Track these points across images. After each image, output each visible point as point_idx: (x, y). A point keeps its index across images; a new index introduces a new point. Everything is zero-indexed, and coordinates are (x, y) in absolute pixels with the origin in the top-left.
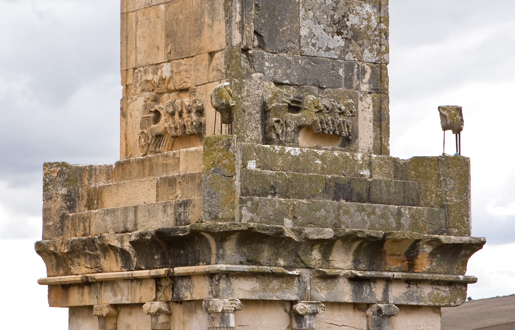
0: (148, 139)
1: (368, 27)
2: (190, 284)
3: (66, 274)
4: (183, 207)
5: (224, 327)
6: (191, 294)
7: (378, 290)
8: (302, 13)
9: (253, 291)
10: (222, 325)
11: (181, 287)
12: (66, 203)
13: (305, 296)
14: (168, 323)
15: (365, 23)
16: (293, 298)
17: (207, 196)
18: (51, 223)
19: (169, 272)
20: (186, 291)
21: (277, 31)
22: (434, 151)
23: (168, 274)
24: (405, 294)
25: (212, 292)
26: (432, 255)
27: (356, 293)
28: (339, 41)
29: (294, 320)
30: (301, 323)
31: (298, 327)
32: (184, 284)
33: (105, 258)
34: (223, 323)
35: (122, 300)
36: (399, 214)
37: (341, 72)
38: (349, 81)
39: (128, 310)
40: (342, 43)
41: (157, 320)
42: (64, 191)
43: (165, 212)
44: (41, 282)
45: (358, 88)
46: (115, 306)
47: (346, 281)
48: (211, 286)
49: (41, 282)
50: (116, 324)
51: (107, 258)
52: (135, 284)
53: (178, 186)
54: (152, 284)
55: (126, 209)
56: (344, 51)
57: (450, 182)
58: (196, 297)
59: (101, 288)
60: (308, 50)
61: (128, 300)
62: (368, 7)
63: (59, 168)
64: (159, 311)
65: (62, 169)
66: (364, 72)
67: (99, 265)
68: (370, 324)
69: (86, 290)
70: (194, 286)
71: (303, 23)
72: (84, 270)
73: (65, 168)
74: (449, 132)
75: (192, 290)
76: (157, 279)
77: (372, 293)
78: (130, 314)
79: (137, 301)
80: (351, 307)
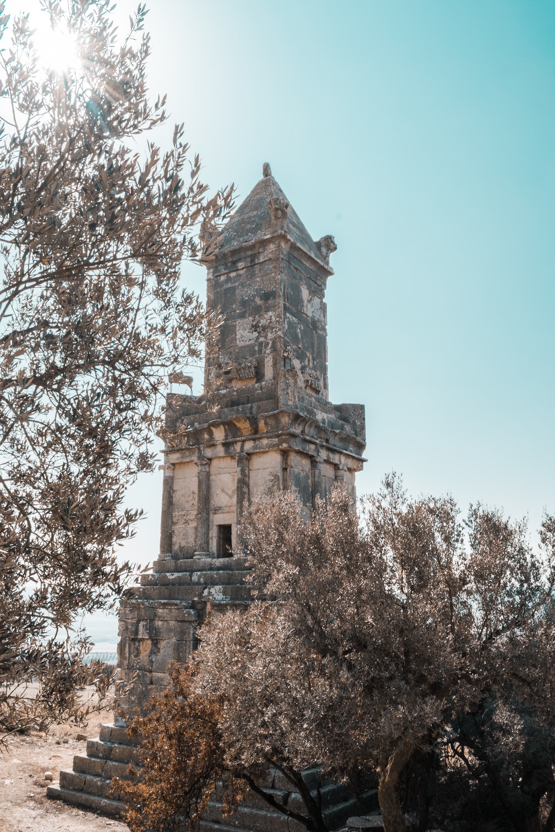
1: (270, 323)
7: (238, 447)
8: (238, 328)
9: (178, 458)
15: (269, 321)
21: (225, 341)
26: (266, 424)
28: (256, 334)
36: (251, 408)
37: (256, 348)
38: (260, 351)
40: (257, 334)
45: (265, 353)
56: (258, 338)
60: (240, 344)
62: (270, 313)
66: (268, 344)
71: (238, 333)
77: (235, 450)
80: (229, 458)
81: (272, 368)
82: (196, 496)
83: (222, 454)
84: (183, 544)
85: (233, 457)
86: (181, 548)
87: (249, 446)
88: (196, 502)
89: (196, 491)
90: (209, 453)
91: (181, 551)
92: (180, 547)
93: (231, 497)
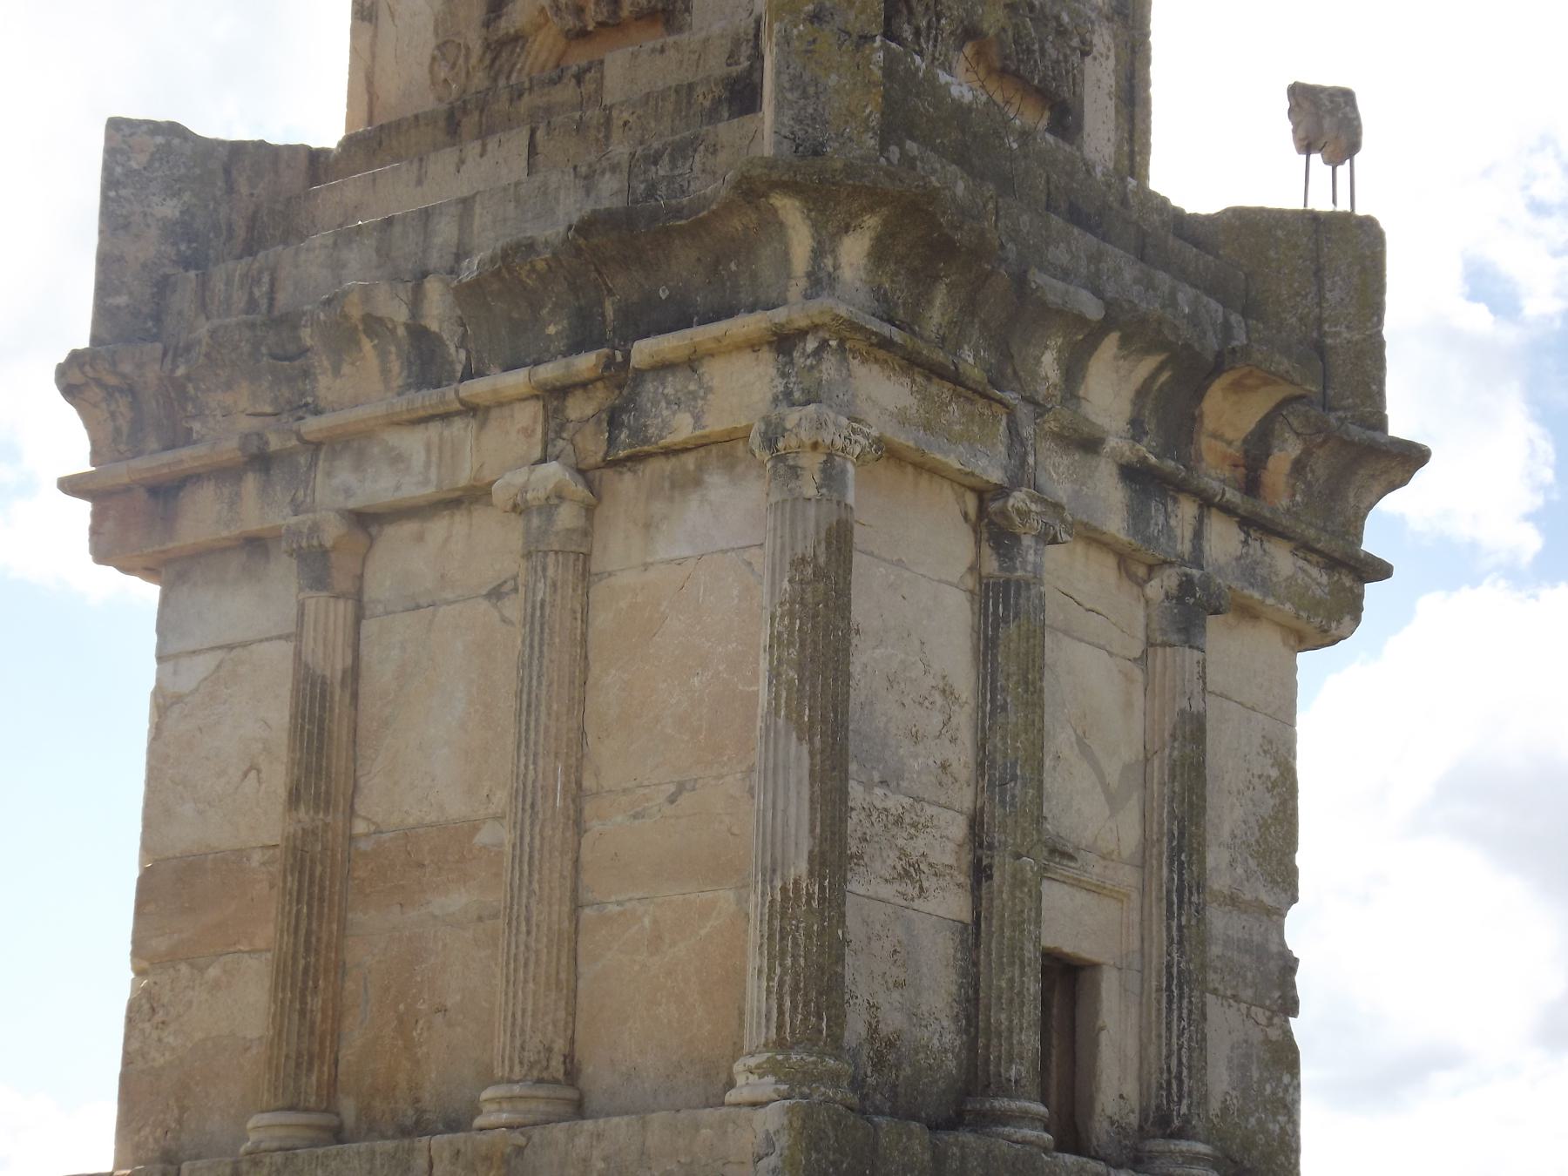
0: (467, 57)
2: (692, 387)
3: (170, 446)
4: (666, 158)
5: (829, 500)
6: (697, 418)
10: (824, 491)
11: (655, 404)
12: (174, 244)
13: (1021, 475)
14: (586, 533)
16: (996, 476)
17: (791, 90)
18: (122, 300)
19: (609, 363)
20: (674, 413)
22: (1287, 198)
23: (607, 367)
24: (1238, 559)
25: (788, 394)
26: (1299, 467)
27: (1137, 517)
29: (987, 550)
30: (1012, 559)
31: (1001, 568)
32: (669, 390)
33: (337, 371)
34: (829, 487)
35: (398, 488)
39: (409, 528)
41: (550, 519)
42: (169, 209)
43: (588, 194)
44: (72, 486)
46: (365, 521)
47: (1115, 470)
48: (784, 375)
49: (72, 486)
50: (361, 577)
51: (346, 369)
52: (458, 424)
53: (616, 134)
54: (529, 415)
55: (426, 215)
57: (1334, 283)
58: (715, 424)
59: (313, 465)
61: (426, 482)
63: (160, 140)
64: (559, 496)
65: (168, 144)
67: (310, 400)
68: (1154, 626)
69: (251, 483)
70: (709, 390)
72: (246, 424)
73: (176, 141)
74: (1316, 158)
75: (700, 402)
76: (555, 395)
77: (1168, 530)
78: (420, 538)
79: (464, 478)
80: (1111, 561)
81: (1111, 104)
82: (963, 719)
83: (1115, 525)
84: (893, 1021)
85: (1123, 559)
86: (883, 1048)
87: (1223, 540)
88: (962, 756)
89: (964, 681)
90: (1058, 474)
91: (879, 1063)
92: (873, 1030)
93: (1114, 802)
